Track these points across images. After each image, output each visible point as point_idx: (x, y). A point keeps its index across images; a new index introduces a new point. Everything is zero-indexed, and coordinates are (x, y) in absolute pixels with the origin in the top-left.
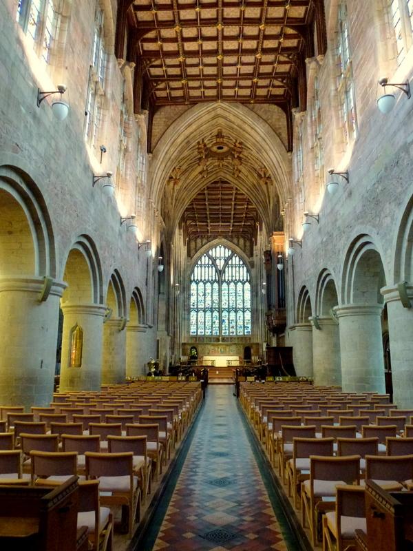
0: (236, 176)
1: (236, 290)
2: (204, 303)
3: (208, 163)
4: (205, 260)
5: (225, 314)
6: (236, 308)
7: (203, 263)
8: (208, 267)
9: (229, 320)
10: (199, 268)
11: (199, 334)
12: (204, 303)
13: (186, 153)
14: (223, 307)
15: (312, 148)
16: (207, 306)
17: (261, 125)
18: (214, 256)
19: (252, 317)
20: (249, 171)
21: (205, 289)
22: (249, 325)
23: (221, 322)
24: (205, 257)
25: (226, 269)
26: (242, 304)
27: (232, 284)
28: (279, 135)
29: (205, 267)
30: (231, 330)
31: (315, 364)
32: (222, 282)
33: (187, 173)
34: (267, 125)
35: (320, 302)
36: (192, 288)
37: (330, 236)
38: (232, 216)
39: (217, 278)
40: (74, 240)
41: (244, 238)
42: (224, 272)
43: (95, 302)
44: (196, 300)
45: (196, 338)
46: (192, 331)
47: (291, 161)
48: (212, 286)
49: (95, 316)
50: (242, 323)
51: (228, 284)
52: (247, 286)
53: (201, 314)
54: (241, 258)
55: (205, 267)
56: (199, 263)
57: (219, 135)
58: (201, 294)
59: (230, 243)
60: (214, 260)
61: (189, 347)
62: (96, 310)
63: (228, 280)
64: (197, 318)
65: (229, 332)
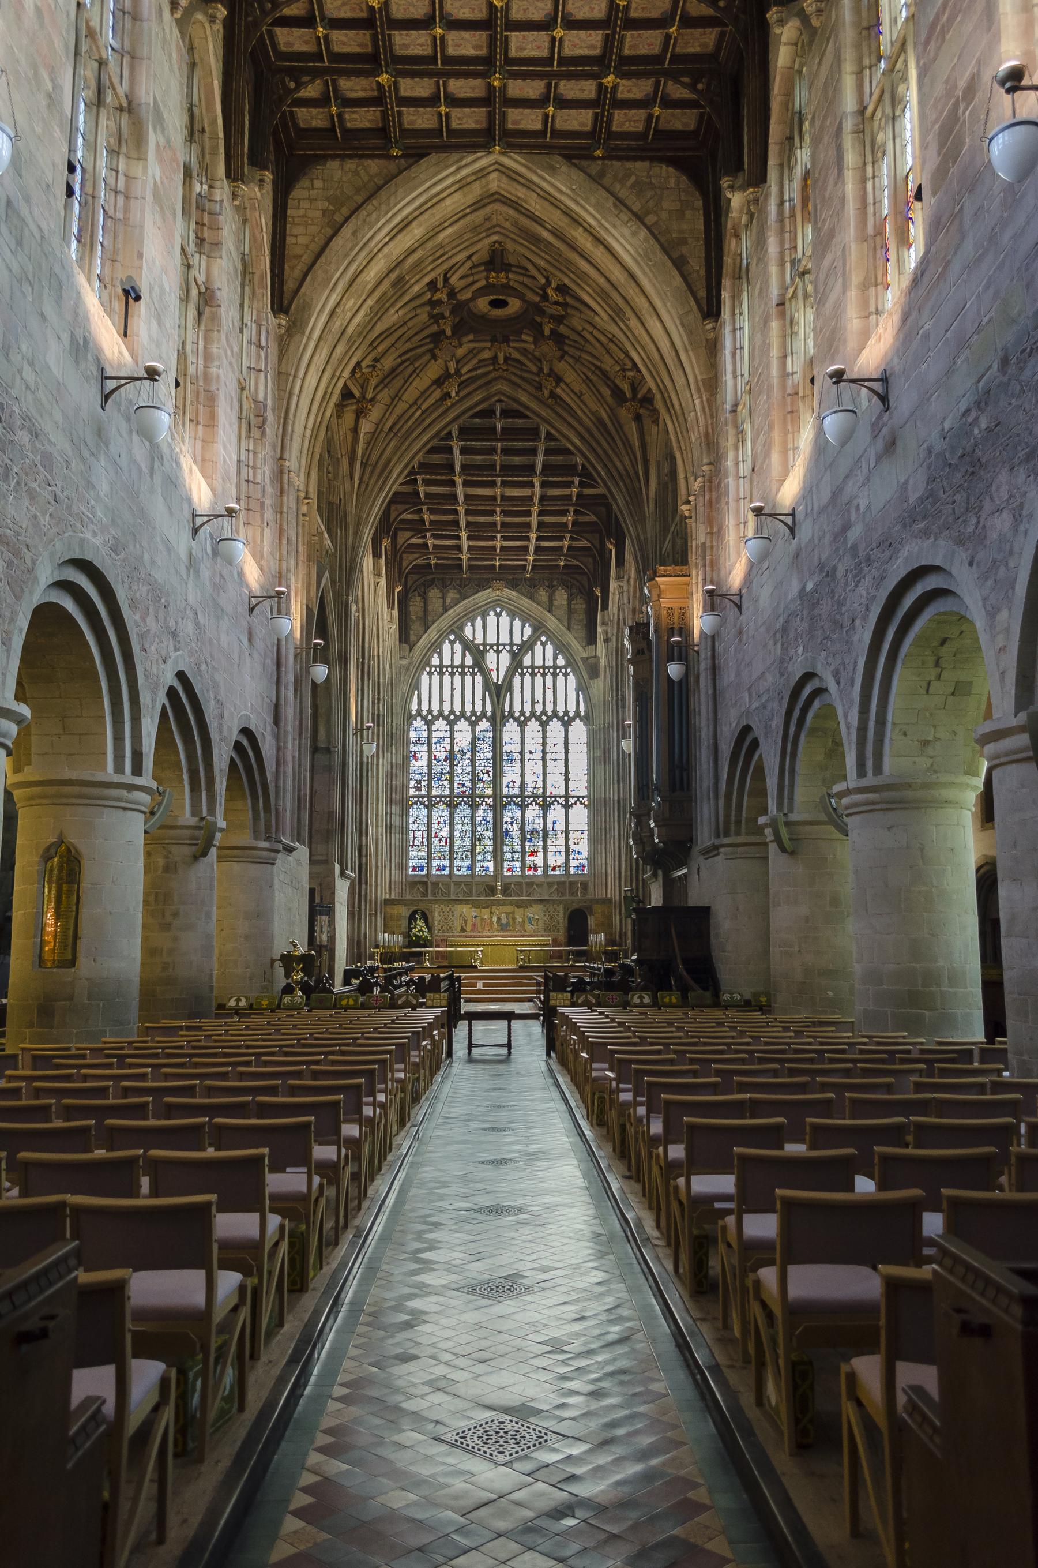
0: (546, 393)
1: (544, 744)
2: (451, 782)
3: (460, 352)
4: (451, 653)
7: (447, 661)
8: (463, 674)
10: (436, 678)
11: (434, 872)
12: (451, 782)
13: (393, 317)
14: (505, 791)
15: (781, 304)
17: (626, 232)
18: (479, 640)
20: (587, 380)
22: (584, 847)
23: (500, 836)
24: (452, 643)
25: (517, 680)
27: (533, 726)
28: (680, 264)
29: (452, 674)
30: (529, 860)
31: (775, 951)
32: (504, 719)
33: (398, 383)
34: (644, 233)
35: (792, 771)
36: (413, 735)
37: (827, 575)
38: (534, 520)
39: (489, 708)
40: (46, 574)
41: (568, 587)
42: (510, 689)
43: (119, 769)
44: (425, 770)
45: (425, 884)
46: (412, 863)
47: (713, 348)
49: (121, 812)
51: (522, 725)
52: (579, 731)
53: (441, 813)
54: (561, 648)
55: (452, 674)
56: (435, 661)
57: (496, 261)
59: (525, 602)
60: (478, 653)
61: (405, 912)
62: (124, 793)
64: (429, 824)
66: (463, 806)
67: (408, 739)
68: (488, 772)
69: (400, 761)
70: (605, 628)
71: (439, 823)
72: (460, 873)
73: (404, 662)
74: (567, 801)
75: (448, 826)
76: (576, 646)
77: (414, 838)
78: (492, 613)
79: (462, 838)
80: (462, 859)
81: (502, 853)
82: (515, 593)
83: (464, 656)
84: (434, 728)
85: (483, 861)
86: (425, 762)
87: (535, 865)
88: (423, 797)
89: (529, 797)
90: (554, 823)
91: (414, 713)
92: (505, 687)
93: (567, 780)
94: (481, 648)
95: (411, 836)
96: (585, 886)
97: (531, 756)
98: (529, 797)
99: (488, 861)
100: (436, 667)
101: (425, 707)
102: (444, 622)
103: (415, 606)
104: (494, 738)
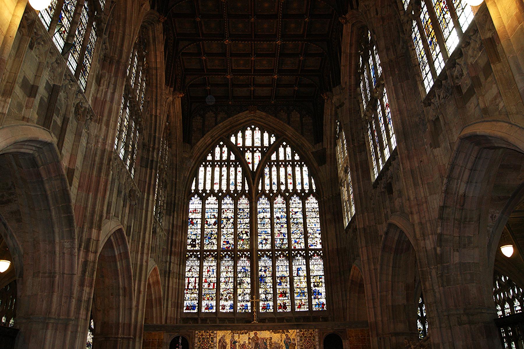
1: (288, 212)
2: (218, 239)
5: (264, 263)
6: (289, 249)
7: (218, 158)
9: (274, 276)
10: (209, 169)
11: (203, 310)
14: (260, 247)
16: (223, 246)
21: (220, 211)
22: (322, 289)
24: (221, 147)
25: (267, 170)
26: (303, 240)
29: (221, 167)
32: (258, 196)
36: (192, 207)
39: (247, 188)
42: (262, 176)
44: (199, 231)
48: (236, 204)
50: (304, 285)
51: (271, 199)
52: (312, 203)
53: (210, 264)
55: (221, 167)
56: (209, 158)
58: (213, 221)
63: (271, 190)
65: (275, 307)
66: (227, 258)
68: (246, 233)
69: (180, 224)
71: (208, 271)
72: (224, 311)
74: (307, 253)
75: (215, 274)
77: (189, 283)
78: (249, 128)
79: (226, 283)
80: (226, 300)
81: (258, 295)
82: (264, 114)
83: (229, 155)
84: (207, 202)
85: (243, 301)
86: (199, 226)
88: (197, 251)
89: (278, 251)
90: (298, 270)
92: (258, 172)
93: (306, 238)
94: (241, 149)
95: (187, 281)
97: (278, 221)
98: (278, 251)
99: (247, 301)
100: (209, 161)
101: (201, 187)
104: (251, 208)
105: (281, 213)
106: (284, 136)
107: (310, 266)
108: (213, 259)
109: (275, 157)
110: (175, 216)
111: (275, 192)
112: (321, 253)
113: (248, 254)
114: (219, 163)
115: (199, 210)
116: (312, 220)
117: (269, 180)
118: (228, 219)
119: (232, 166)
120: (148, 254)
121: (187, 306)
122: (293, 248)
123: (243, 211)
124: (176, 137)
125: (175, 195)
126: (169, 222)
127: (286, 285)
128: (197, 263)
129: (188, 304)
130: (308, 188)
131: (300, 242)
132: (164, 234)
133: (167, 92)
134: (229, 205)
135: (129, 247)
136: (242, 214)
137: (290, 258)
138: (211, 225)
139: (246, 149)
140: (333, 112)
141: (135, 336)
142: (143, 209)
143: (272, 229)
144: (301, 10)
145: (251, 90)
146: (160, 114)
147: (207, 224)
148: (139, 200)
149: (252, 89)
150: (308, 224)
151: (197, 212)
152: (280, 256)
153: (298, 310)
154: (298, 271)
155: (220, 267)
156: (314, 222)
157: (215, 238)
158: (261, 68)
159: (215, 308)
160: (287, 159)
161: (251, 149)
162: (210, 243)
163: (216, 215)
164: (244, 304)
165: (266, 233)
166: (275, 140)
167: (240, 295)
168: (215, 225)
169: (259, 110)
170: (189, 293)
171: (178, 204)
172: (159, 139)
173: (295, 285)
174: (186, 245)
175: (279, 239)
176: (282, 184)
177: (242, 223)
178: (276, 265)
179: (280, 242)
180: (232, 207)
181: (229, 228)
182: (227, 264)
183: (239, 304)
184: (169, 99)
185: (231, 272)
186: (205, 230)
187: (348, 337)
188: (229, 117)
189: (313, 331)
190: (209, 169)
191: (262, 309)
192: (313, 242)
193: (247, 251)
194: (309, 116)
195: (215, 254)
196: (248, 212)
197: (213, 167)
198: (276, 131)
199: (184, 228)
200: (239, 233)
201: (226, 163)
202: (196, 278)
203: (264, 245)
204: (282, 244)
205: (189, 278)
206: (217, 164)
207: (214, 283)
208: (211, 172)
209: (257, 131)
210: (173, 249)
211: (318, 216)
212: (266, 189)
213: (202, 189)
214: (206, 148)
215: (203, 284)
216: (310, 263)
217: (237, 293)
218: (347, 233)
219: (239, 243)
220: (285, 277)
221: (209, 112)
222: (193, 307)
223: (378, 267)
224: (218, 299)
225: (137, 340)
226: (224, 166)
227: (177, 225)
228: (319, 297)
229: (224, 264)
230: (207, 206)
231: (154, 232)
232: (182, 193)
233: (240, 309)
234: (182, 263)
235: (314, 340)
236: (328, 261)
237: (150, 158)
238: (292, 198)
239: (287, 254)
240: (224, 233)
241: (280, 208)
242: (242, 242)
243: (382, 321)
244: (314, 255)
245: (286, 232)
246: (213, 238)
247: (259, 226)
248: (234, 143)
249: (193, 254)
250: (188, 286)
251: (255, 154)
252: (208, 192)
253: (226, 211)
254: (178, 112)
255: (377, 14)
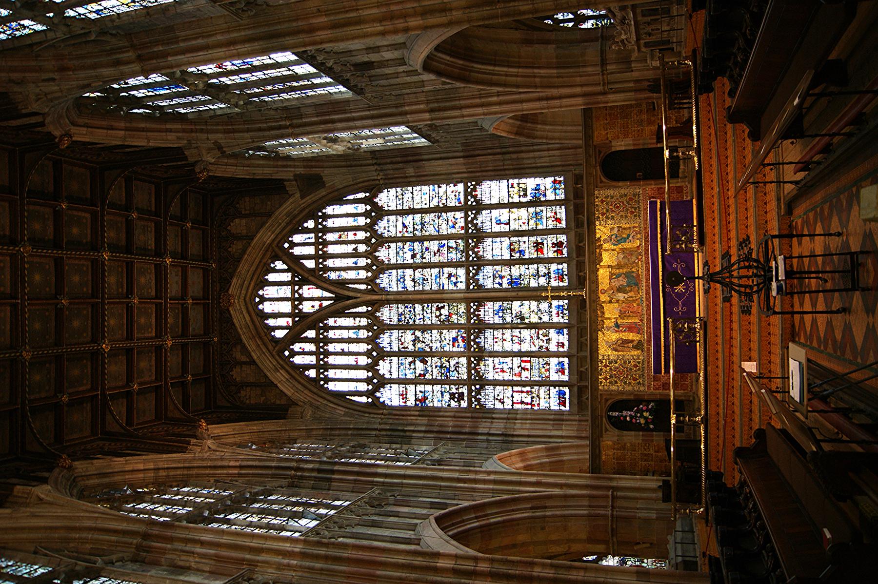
1: (404, 240)
2: (450, 355)
5: (487, 278)
6: (465, 237)
7: (311, 360)
9: (509, 263)
10: (331, 373)
11: (565, 378)
14: (462, 286)
16: (461, 347)
19: (498, 175)
21: (402, 353)
22: (531, 183)
25: (333, 276)
26: (450, 215)
29: (327, 354)
36: (396, 402)
39: (363, 309)
44: (437, 388)
46: (555, 406)
48: (391, 327)
50: (523, 212)
51: (381, 267)
52: (387, 198)
53: (490, 369)
55: (327, 354)
56: (312, 373)
58: (419, 366)
59: (244, 268)
63: (367, 268)
66: (481, 340)
67: (399, 408)
68: (439, 309)
69: (424, 420)
70: (204, 152)
71: (503, 371)
72: (566, 344)
73: (309, 413)
74: (471, 208)
75: (508, 360)
76: (288, 206)
77: (522, 402)
78: (261, 307)
79: (521, 341)
80: (548, 341)
82: (234, 280)
84: (387, 376)
86: (428, 388)
87: (554, 245)
88: (470, 391)
89: (468, 256)
90: (499, 222)
91: (370, 400)
92: (337, 290)
93: (447, 209)
94: (297, 319)
96: (578, 179)
97: (418, 256)
98: (468, 256)
100: (318, 373)
101: (363, 387)
102: (267, 363)
103: (251, 397)
104: (397, 302)
105: (404, 250)
106: (274, 246)
107: (492, 203)
108: (482, 364)
109: (309, 261)
110: (412, 428)
111: (369, 261)
112: (472, 185)
113: (474, 305)
114: (322, 357)
115: (401, 389)
116: (417, 199)
117: (349, 272)
118: (416, 340)
119: (325, 334)
120: (476, 472)
121: (559, 404)
122: (463, 232)
123: (402, 314)
124: (277, 431)
125: (376, 429)
126: (422, 438)
127: (525, 242)
128: (489, 389)
129: (556, 404)
130: (363, 205)
131: (454, 220)
132: (442, 445)
133: (198, 449)
134: (393, 338)
135: (466, 504)
136: (407, 316)
137: (480, 236)
138: (426, 368)
139: (297, 311)
140: (232, 161)
141: (608, 488)
142: (402, 484)
143: (431, 266)
144: (47, 216)
145: (193, 304)
146: (237, 460)
147: (424, 375)
148: (386, 491)
149: (190, 301)
150: (424, 206)
151: (405, 393)
152: (476, 253)
153: (564, 222)
154: (500, 223)
155: (496, 352)
156: (420, 195)
157: (448, 361)
158: (153, 286)
159: (561, 359)
160: (313, 240)
161: (296, 303)
162: (456, 369)
163: (410, 359)
164: (554, 311)
165: (439, 276)
166: (281, 262)
167: (541, 319)
168: (427, 362)
169: (228, 290)
170: (538, 402)
171: (391, 424)
172: (282, 459)
173: (524, 228)
174: (460, 410)
175: (449, 255)
176: (355, 249)
177: (422, 317)
178: (491, 258)
179: (454, 252)
180: (395, 333)
181: (430, 338)
182: (490, 341)
183: (556, 320)
184: (210, 446)
185: (503, 334)
186: (434, 377)
187: (607, 141)
188: (241, 340)
189: (597, 198)
190: (331, 373)
191: (563, 281)
192: (454, 198)
193: (468, 308)
194: (238, 203)
195: (475, 360)
196: (403, 307)
197: (327, 367)
198: (264, 261)
199: (431, 413)
200: (440, 321)
201: (321, 345)
202: (513, 391)
203: (459, 280)
204: (456, 248)
205: (513, 403)
206: (322, 360)
207: (522, 361)
208: (337, 370)
209: (265, 293)
210: (467, 430)
211: (410, 188)
212: (365, 277)
213: (365, 384)
214: (296, 380)
215: (523, 379)
216: (488, 202)
217: (538, 323)
218: (437, 141)
219: (456, 321)
220: (511, 244)
221: (232, 376)
222: (561, 394)
223: (495, 89)
224: (548, 353)
225: (614, 484)
226: (325, 347)
227: (427, 425)
228: (542, 188)
229: (490, 346)
230: (395, 376)
231: (439, 462)
232: (373, 417)
233: (563, 317)
234: (490, 415)
235: (612, 197)
236: (484, 174)
237: (314, 474)
238: (379, 232)
239: (473, 241)
240: (439, 346)
241: (398, 253)
242: (454, 317)
243: (582, 86)
244: (475, 197)
245: (436, 242)
246: (448, 364)
247: (427, 288)
248: (286, 331)
249: (475, 397)
250: (527, 404)
251: (305, 295)
252: (370, 374)
253: (402, 344)
254: (234, 430)
255: (53, 80)
